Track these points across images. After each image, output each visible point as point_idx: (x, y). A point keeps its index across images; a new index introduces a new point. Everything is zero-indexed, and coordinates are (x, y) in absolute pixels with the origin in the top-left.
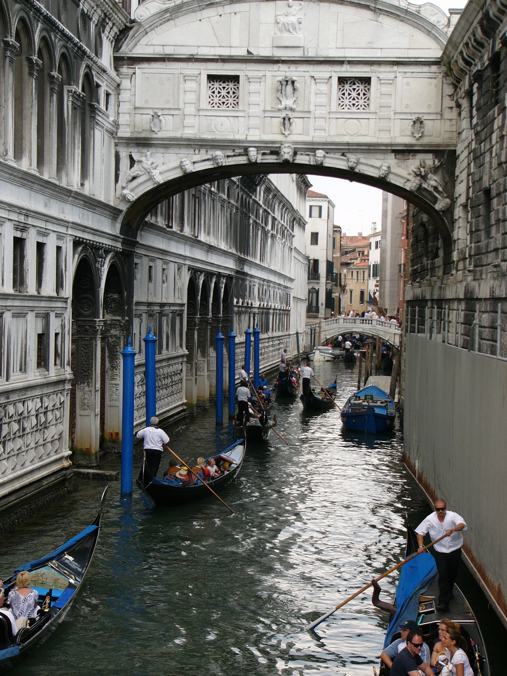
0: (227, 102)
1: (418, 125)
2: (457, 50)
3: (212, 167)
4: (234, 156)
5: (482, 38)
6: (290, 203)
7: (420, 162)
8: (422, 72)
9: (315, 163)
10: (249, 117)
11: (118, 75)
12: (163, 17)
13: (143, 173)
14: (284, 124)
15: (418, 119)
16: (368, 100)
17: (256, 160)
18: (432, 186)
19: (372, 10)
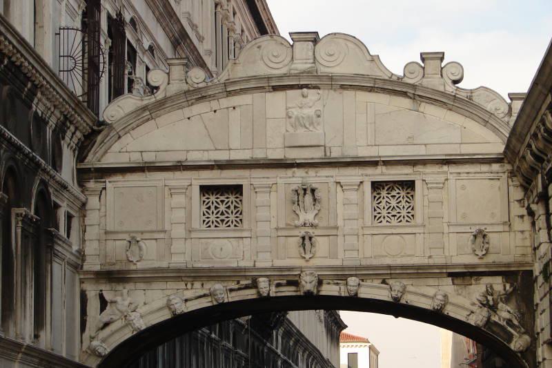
0: (227, 220)
1: (480, 240)
2: (522, 143)
3: (210, 304)
4: (239, 289)
6: (318, 351)
7: (487, 287)
8: (481, 173)
9: (347, 295)
10: (257, 237)
11: (83, 192)
12: (141, 116)
13: (118, 317)
14: (303, 245)
15: (480, 232)
16: (413, 209)
17: (269, 294)
18: (504, 320)
19: (411, 98)
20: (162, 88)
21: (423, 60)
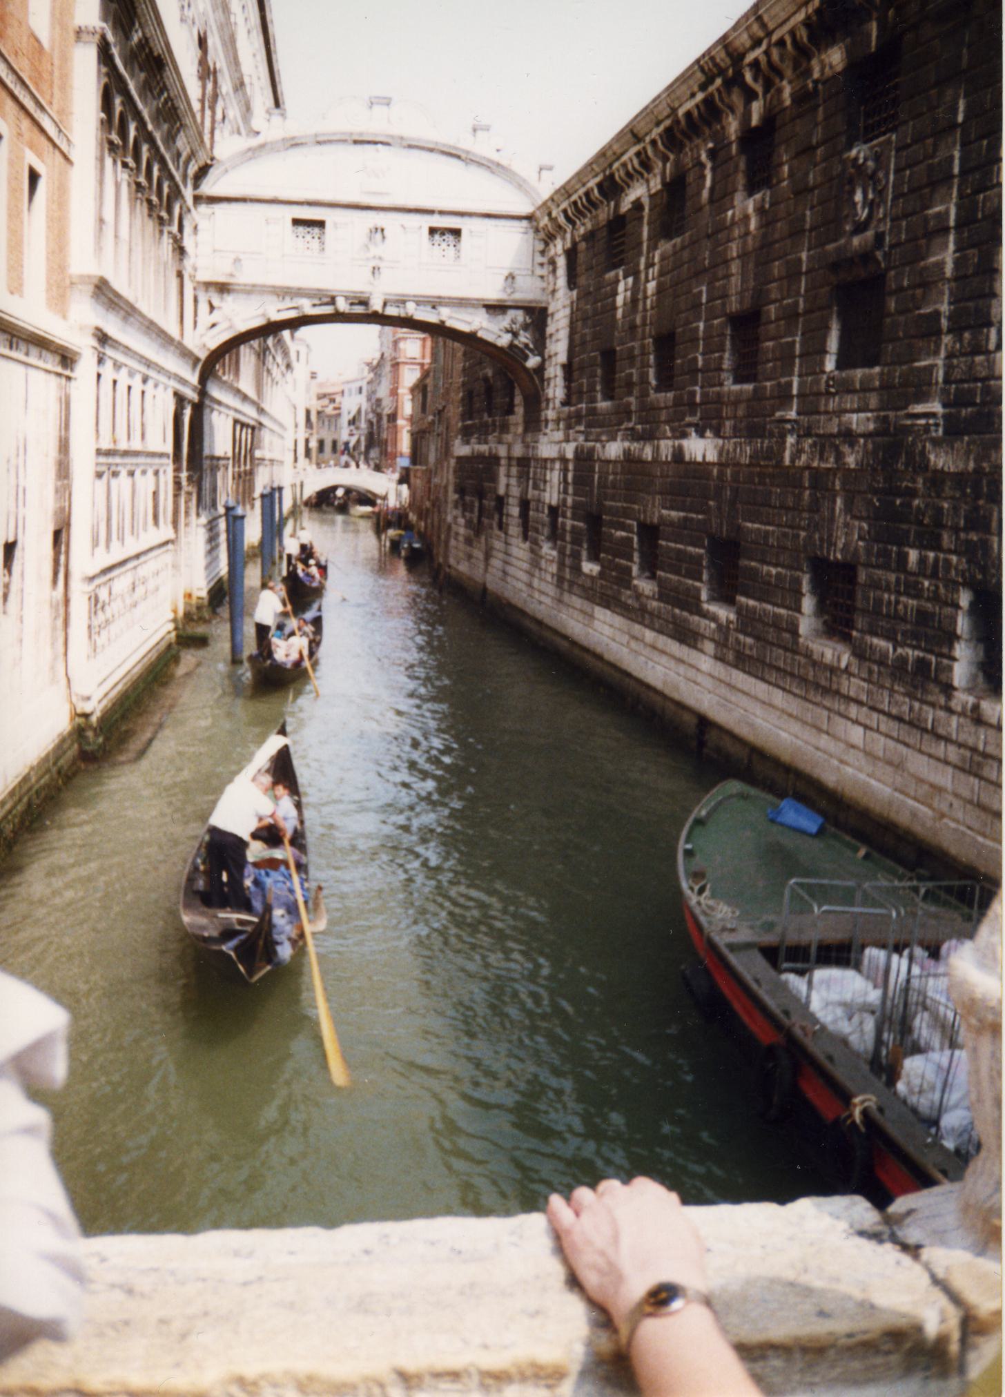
21: (475, 130)
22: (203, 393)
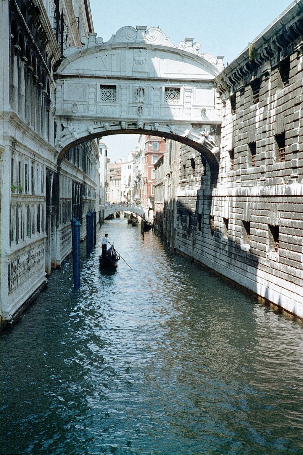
3: (103, 131)
4: (114, 125)
5: (245, 71)
9: (154, 130)
10: (121, 106)
14: (139, 110)
20: (86, 45)
22: (59, 168)
